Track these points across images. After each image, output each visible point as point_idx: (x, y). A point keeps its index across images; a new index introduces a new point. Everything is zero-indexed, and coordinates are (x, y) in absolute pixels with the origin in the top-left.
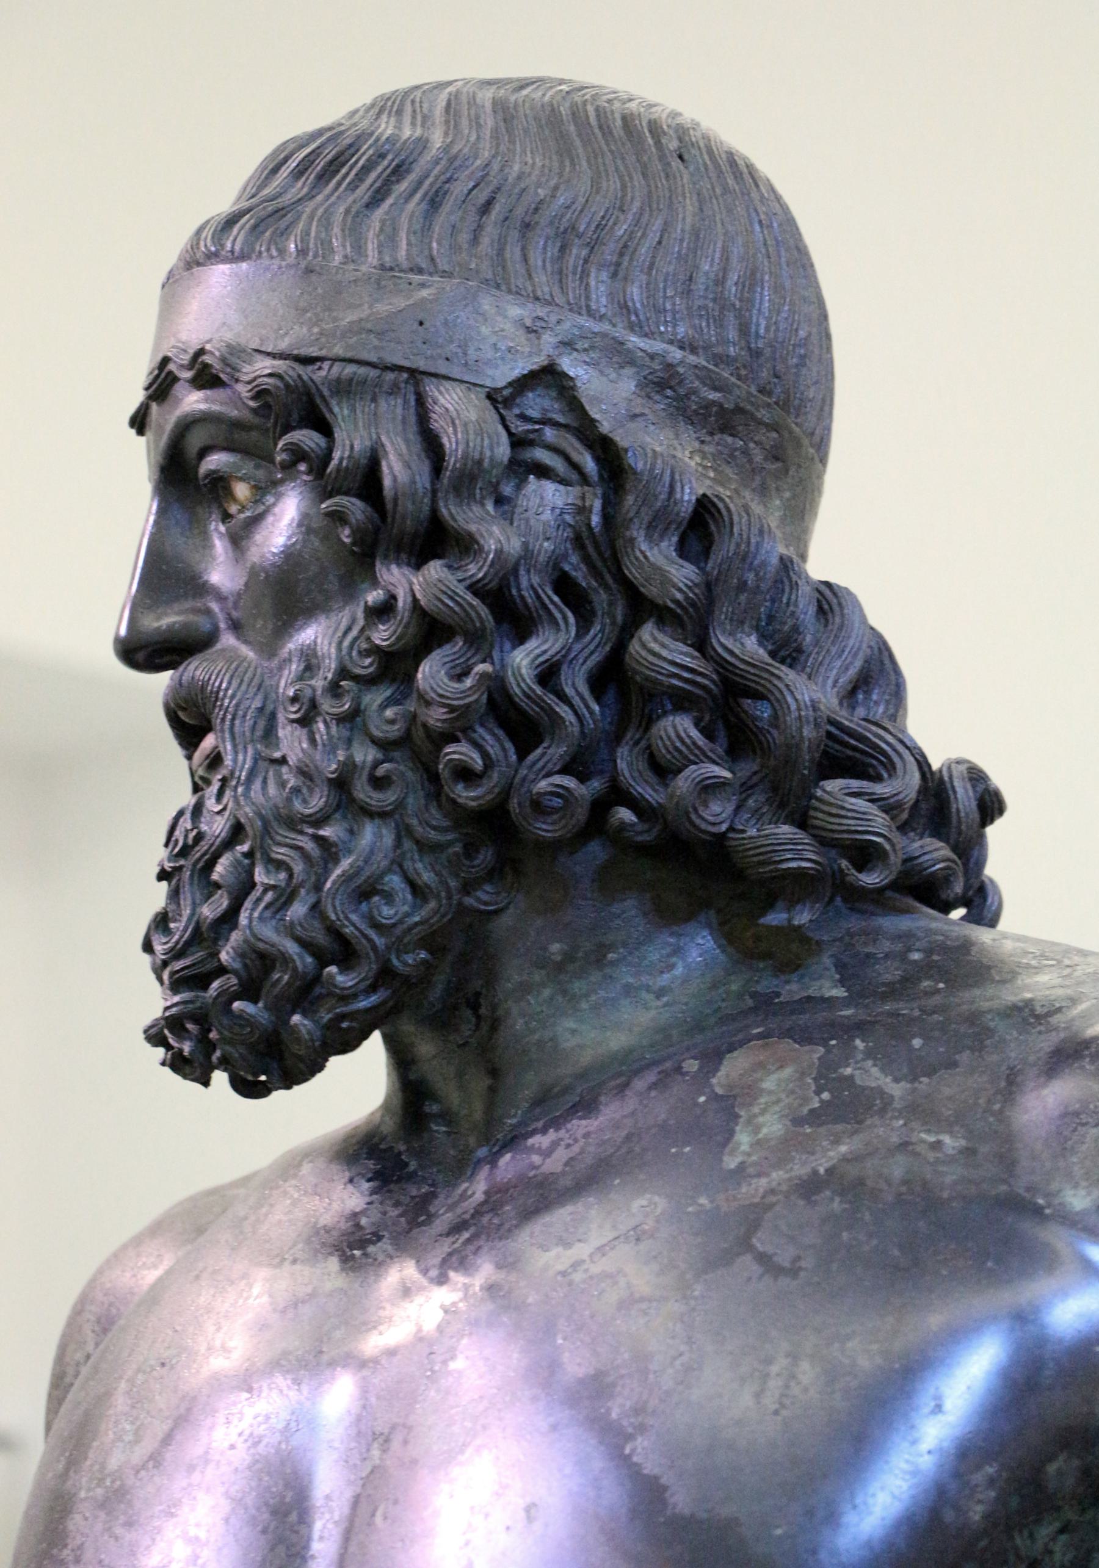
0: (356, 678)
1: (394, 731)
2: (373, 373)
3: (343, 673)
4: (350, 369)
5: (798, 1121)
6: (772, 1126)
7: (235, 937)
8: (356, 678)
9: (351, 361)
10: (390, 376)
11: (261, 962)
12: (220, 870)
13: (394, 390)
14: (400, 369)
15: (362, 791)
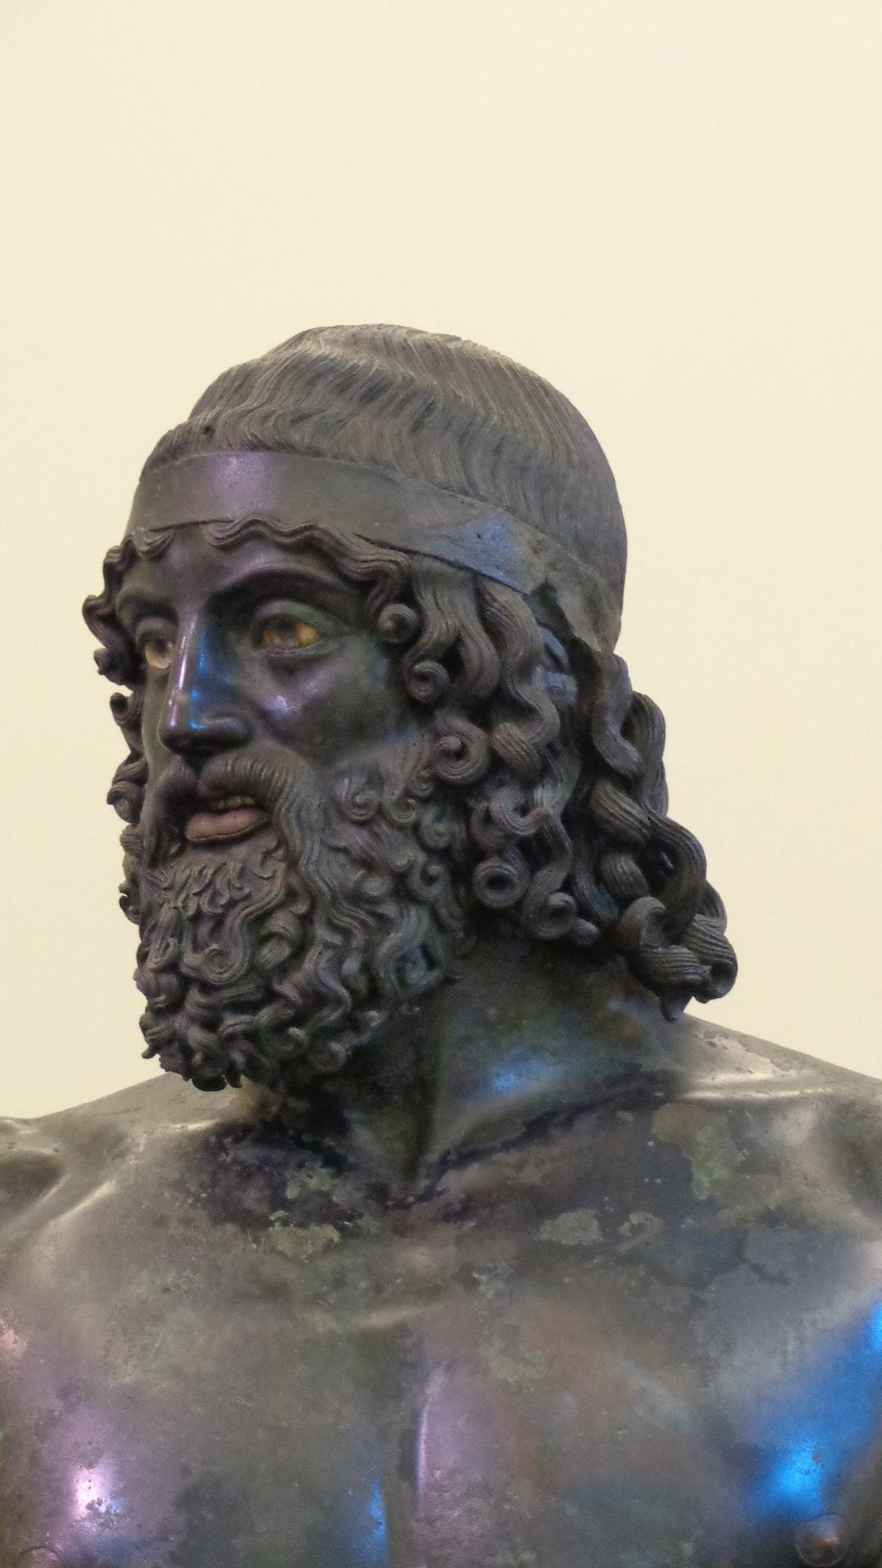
0: (416, 798)
1: (442, 843)
2: (451, 570)
3: (407, 793)
4: (437, 565)
5: (737, 1170)
6: (722, 1173)
7: (298, 977)
8: (416, 798)
9: (436, 558)
10: (461, 574)
11: (317, 998)
12: (281, 922)
13: (462, 586)
14: (467, 569)
15: (415, 882)
